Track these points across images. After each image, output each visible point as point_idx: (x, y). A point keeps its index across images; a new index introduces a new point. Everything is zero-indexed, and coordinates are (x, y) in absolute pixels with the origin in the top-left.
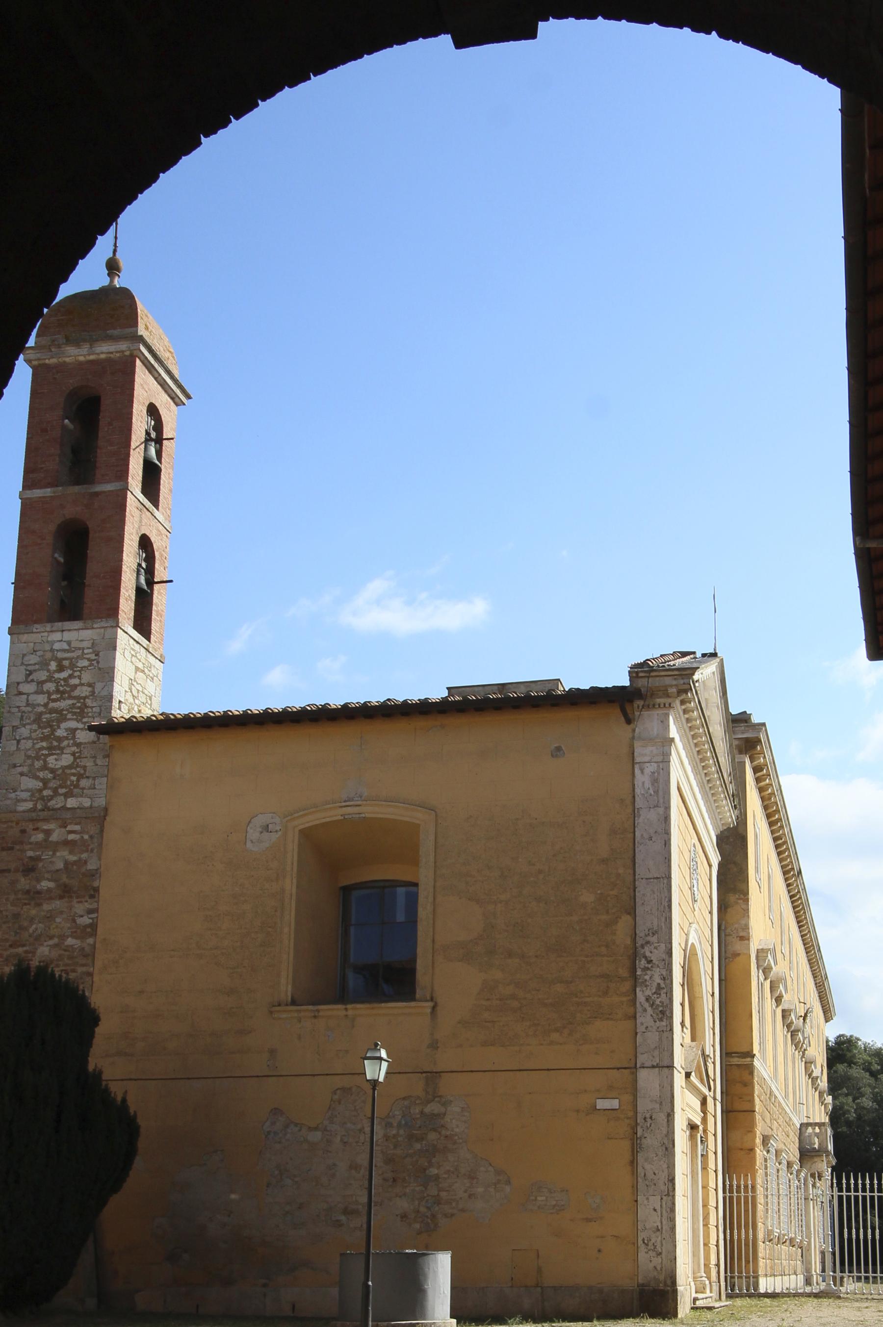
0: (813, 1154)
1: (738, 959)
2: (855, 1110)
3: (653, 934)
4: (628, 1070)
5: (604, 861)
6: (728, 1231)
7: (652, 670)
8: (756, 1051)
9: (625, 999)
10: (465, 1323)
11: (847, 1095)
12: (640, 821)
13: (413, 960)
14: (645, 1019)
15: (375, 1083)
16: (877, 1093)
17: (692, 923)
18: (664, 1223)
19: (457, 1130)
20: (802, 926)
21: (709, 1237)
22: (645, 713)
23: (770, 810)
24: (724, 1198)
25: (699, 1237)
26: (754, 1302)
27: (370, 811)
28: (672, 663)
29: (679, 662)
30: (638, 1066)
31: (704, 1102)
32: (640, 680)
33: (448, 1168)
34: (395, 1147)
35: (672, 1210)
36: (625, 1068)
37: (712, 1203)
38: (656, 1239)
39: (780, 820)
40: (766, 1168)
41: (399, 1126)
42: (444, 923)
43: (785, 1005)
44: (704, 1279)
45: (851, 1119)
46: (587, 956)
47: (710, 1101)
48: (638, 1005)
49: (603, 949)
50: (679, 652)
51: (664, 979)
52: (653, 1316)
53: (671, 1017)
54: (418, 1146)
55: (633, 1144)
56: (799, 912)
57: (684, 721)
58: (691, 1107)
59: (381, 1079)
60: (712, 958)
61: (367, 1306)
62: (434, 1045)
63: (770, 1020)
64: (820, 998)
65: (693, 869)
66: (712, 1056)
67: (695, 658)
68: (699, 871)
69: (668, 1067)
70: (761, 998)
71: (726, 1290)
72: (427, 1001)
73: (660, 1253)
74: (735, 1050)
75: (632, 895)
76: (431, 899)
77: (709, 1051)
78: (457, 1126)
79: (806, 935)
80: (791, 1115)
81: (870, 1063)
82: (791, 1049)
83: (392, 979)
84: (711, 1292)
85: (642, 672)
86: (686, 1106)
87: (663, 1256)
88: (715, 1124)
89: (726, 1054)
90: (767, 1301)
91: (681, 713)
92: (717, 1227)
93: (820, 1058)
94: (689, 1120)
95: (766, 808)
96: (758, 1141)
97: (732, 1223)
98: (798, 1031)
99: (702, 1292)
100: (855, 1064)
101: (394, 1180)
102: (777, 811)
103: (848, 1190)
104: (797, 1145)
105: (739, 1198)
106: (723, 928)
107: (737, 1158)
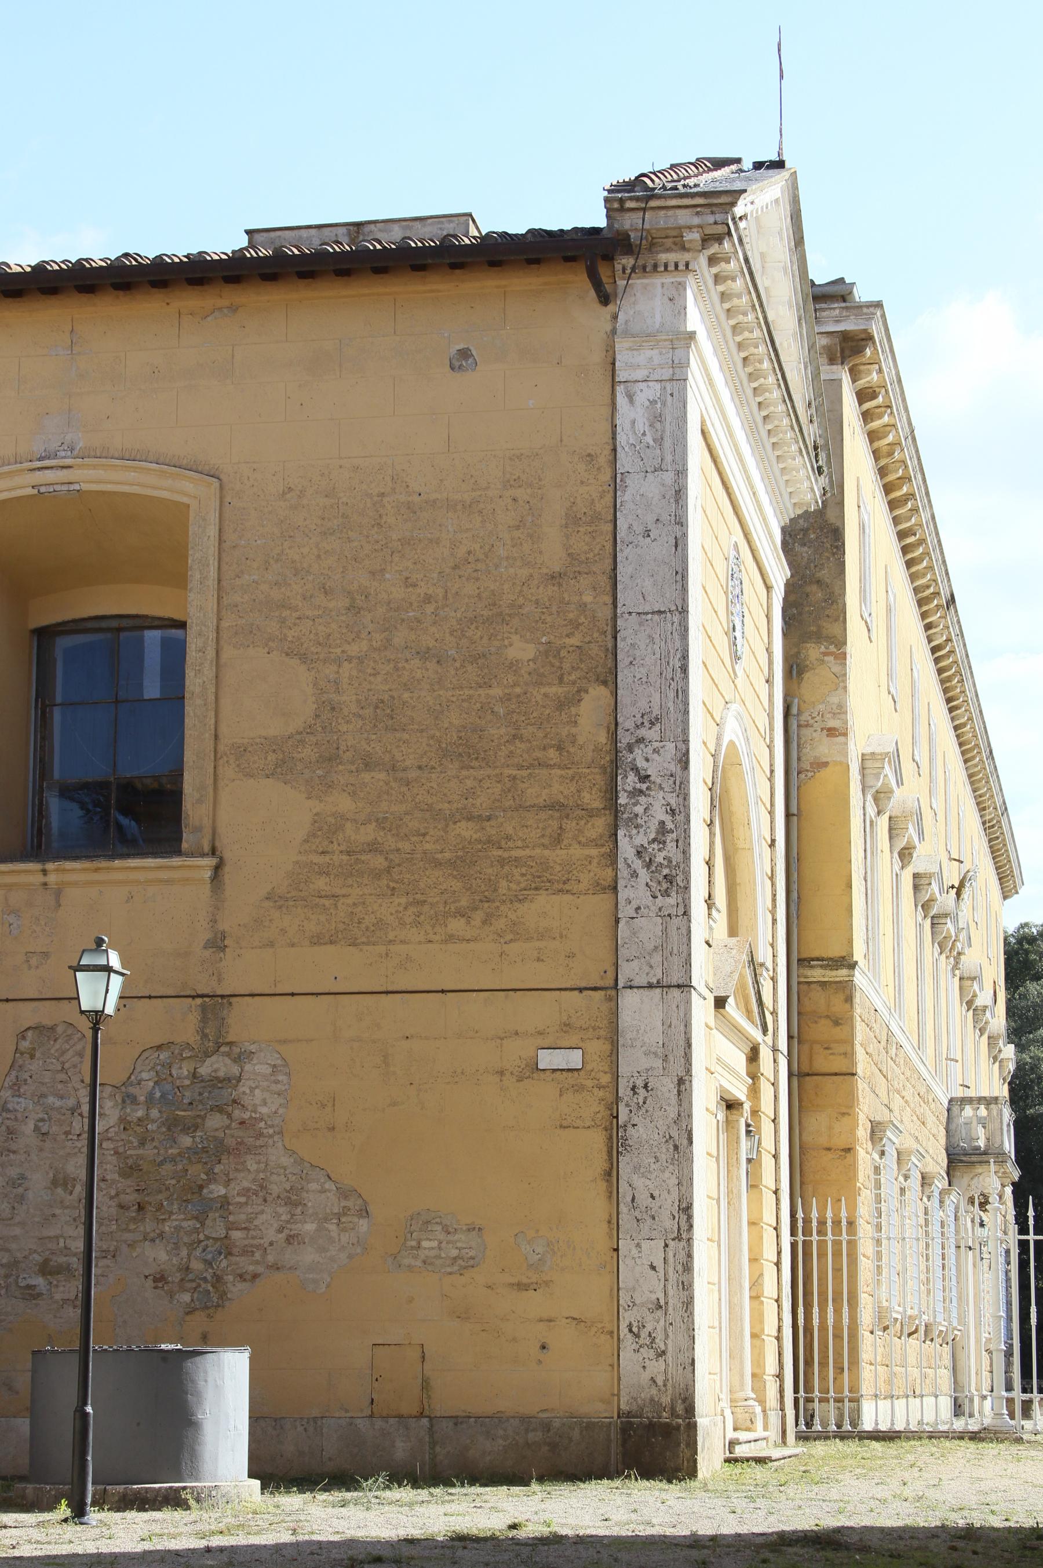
0: (974, 1158)
1: (824, 773)
3: (652, 723)
4: (602, 993)
5: (555, 578)
6: (801, 1310)
7: (651, 195)
8: (858, 955)
9: (594, 852)
10: (278, 1487)
12: (625, 497)
13: (178, 775)
14: (635, 891)
15: (97, 1017)
17: (728, 701)
18: (671, 1292)
19: (264, 1110)
20: (956, 708)
21: (762, 1322)
22: (637, 282)
24: (794, 1246)
26: (852, 1447)
27: (90, 478)
28: (691, 182)
29: (706, 181)
30: (621, 984)
31: (753, 1056)
32: (627, 215)
33: (246, 1184)
34: (142, 1144)
36: (595, 989)
38: (654, 1323)
40: (878, 1185)
43: (918, 864)
44: (751, 1402)
46: (520, 767)
47: (765, 1054)
48: (621, 865)
49: (552, 753)
50: (709, 160)
52: (647, 1474)
53: (687, 888)
54: (186, 1141)
55: (611, 1138)
57: (716, 299)
58: (727, 1067)
59: (110, 1010)
60: (772, 771)
61: (84, 1453)
62: (218, 943)
63: (888, 894)
64: (993, 850)
65: (735, 598)
67: (742, 171)
69: (679, 986)
71: (797, 1425)
72: (203, 855)
73: (664, 1353)
74: (816, 954)
75: (610, 645)
76: (211, 653)
77: (764, 955)
78: (265, 1103)
79: (964, 725)
80: (930, 1080)
82: (930, 951)
83: (139, 814)
85: (631, 199)
86: (716, 1062)
87: (669, 1354)
88: (775, 1098)
89: (799, 961)
91: (710, 281)
93: (993, 971)
94: (723, 1089)
95: (882, 472)
96: (863, 1132)
97: (808, 1294)
99: (748, 1429)
101: (141, 1208)
102: (906, 479)
104: (943, 1140)
105: (822, 1244)
106: (794, 710)
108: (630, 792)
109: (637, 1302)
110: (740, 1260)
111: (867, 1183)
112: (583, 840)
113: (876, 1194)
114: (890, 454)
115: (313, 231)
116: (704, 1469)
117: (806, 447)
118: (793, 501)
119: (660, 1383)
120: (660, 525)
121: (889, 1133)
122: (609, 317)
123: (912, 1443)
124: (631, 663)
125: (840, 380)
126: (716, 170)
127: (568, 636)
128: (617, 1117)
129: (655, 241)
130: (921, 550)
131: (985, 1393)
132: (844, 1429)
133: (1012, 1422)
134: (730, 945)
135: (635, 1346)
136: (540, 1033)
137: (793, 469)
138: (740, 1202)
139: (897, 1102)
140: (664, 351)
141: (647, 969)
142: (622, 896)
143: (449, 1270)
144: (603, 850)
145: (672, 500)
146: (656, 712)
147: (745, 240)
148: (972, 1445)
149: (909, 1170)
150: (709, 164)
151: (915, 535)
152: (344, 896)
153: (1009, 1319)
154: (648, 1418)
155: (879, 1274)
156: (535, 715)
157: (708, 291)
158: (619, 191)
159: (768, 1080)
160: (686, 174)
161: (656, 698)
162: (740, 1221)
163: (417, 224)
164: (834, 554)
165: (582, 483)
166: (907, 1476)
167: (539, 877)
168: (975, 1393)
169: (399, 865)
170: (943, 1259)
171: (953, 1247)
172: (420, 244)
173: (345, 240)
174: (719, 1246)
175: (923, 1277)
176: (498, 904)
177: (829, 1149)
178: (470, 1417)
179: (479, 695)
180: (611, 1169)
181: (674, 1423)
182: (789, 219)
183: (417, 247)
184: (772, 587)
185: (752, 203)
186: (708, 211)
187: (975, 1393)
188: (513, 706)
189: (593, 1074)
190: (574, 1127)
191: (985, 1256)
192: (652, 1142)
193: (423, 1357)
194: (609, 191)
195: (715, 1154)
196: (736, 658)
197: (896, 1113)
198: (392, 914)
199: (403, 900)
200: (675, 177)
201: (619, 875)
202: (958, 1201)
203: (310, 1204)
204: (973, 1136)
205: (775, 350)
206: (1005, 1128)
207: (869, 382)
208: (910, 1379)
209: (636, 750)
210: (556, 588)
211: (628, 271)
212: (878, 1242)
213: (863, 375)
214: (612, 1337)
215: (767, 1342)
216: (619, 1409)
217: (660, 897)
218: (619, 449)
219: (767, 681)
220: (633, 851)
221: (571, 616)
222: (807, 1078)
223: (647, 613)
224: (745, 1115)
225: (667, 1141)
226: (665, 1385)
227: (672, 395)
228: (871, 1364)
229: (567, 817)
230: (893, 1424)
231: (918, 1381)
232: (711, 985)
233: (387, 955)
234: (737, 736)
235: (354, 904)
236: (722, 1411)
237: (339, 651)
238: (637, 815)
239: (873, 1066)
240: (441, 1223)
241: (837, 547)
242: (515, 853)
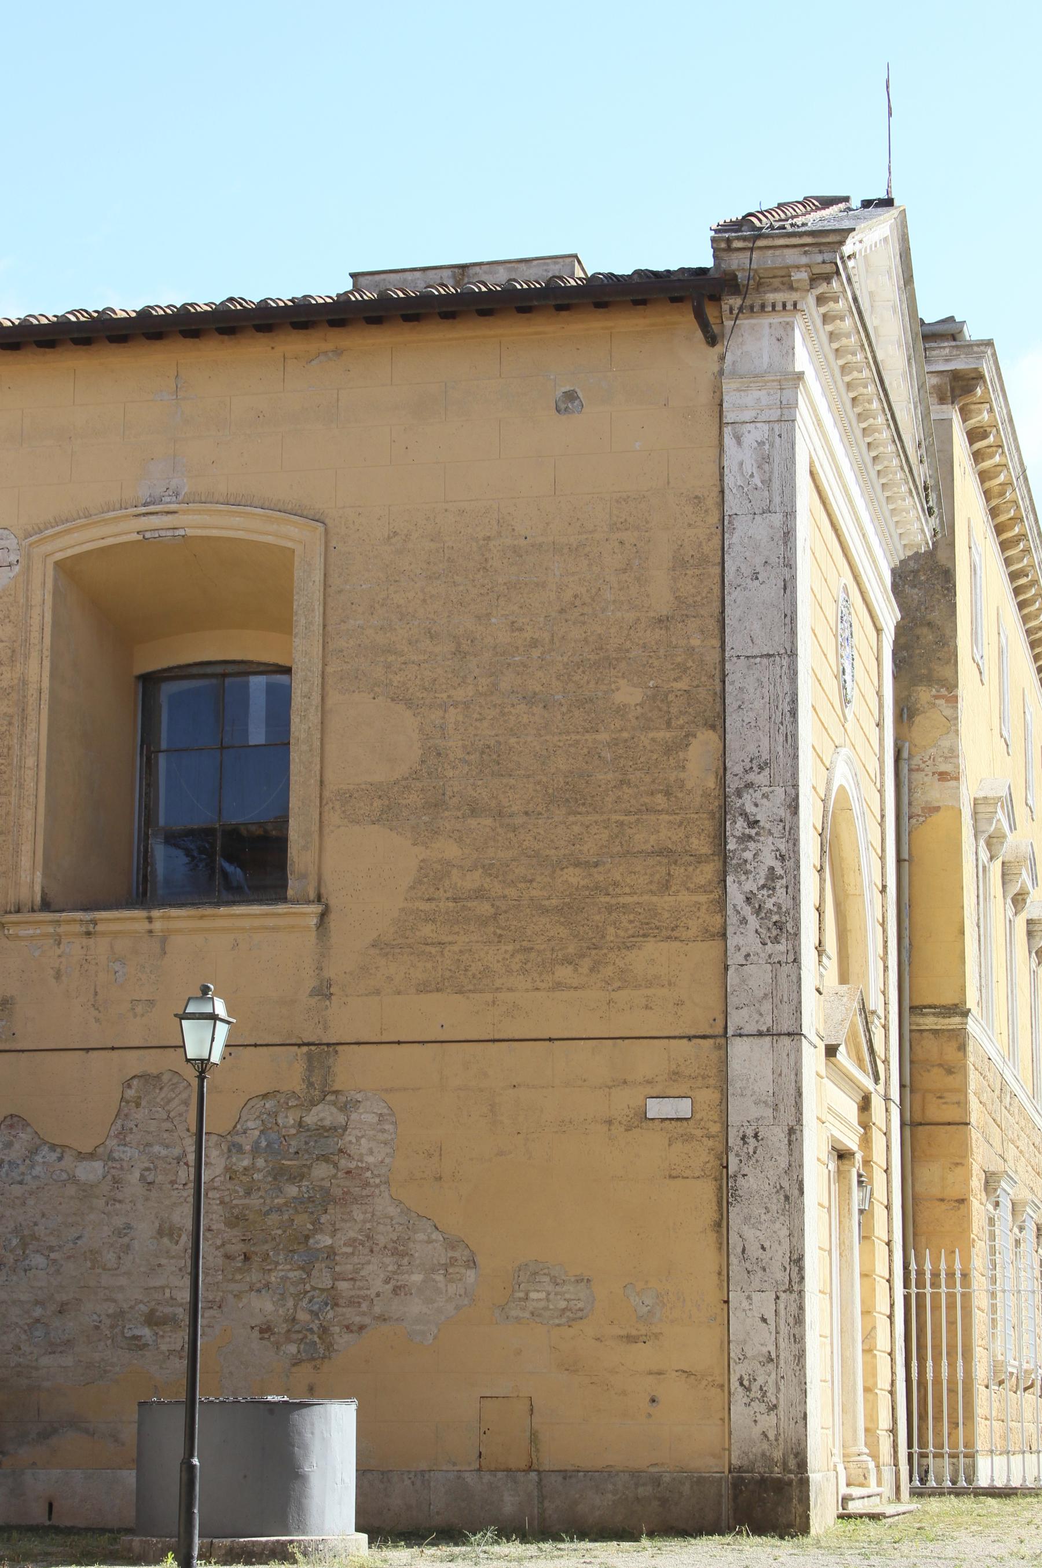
1: (936, 818)
3: (761, 768)
4: (711, 1041)
5: (662, 622)
6: (914, 1363)
7: (758, 234)
8: (971, 1003)
9: (703, 898)
10: (386, 1542)
13: (283, 822)
14: (744, 938)
15: (203, 1066)
17: (838, 746)
18: (782, 1345)
19: (370, 1159)
21: (874, 1375)
22: (745, 322)
23: (1003, 518)
24: (907, 1298)
26: (967, 1503)
27: (195, 523)
28: (799, 221)
29: (814, 220)
30: (730, 1032)
31: (865, 1105)
33: (352, 1234)
35: (799, 1320)
36: (704, 1037)
38: (765, 1377)
39: (1023, 536)
40: (992, 1237)
41: (256, 1150)
42: (342, 748)
44: (865, 1458)
46: (628, 813)
47: (877, 1104)
48: (730, 911)
49: (660, 799)
50: (817, 198)
51: (782, 858)
52: (759, 1529)
53: (797, 935)
54: (292, 1191)
55: (720, 1188)
57: (825, 339)
58: (837, 1116)
59: (216, 1058)
60: (883, 816)
62: (323, 991)
65: (844, 640)
66: (881, 1012)
67: (851, 209)
68: (855, 640)
69: (789, 1034)
71: (911, 1481)
72: (309, 902)
73: (775, 1407)
75: (718, 689)
77: (875, 1002)
78: (371, 1152)
83: (245, 861)
84: (879, 1484)
85: (738, 238)
86: (827, 1110)
87: (781, 1408)
88: (887, 1148)
89: (911, 1008)
90: (990, 1501)
91: (819, 321)
95: (994, 512)
96: (976, 1183)
97: (922, 1347)
101: (247, 1258)
102: (1018, 519)
105: (935, 1297)
106: (905, 754)
108: (739, 837)
110: (852, 1313)
111: (981, 1235)
112: (692, 886)
113: (991, 1246)
114: (1002, 494)
115: (418, 274)
117: (916, 488)
118: (903, 542)
119: (772, 1437)
120: (769, 568)
121: (1003, 1184)
122: (716, 358)
123: (1029, 1499)
125: (951, 420)
126: (824, 209)
127: (675, 680)
128: (727, 1167)
130: (1033, 591)
132: (959, 1485)
134: (841, 993)
135: (746, 1400)
136: (648, 1082)
137: (903, 510)
138: (852, 1254)
139: (1011, 1152)
141: (756, 1017)
142: (731, 942)
143: (557, 1321)
144: (712, 896)
145: (781, 542)
146: (765, 756)
147: (854, 279)
149: (1024, 1221)
150: (816, 203)
151: (1027, 576)
152: (450, 943)
154: (759, 1473)
155: (994, 1327)
156: (642, 760)
157: (817, 332)
158: (726, 231)
159: (880, 1130)
160: (794, 213)
161: (765, 742)
162: (852, 1272)
163: (523, 266)
164: (945, 596)
165: (690, 525)
166: (1023, 1533)
167: (647, 924)
169: (506, 912)
172: (525, 286)
173: (450, 282)
174: (831, 1298)
176: (606, 951)
177: (942, 1200)
178: (579, 1471)
180: (721, 1219)
181: (786, 1478)
182: (898, 257)
183: (523, 289)
185: (861, 242)
188: (621, 751)
189: (702, 1123)
190: (683, 1178)
192: (762, 1192)
193: (532, 1410)
194: (716, 231)
195: (827, 1205)
197: (1011, 1163)
198: (498, 961)
199: (510, 948)
200: (783, 216)
203: (417, 1255)
205: (885, 390)
209: (745, 795)
210: (663, 632)
211: (736, 312)
213: (974, 415)
214: (723, 1391)
216: (730, 1464)
217: (770, 944)
218: (727, 491)
219: (878, 725)
220: (742, 897)
221: (679, 659)
222: (920, 1128)
223: (755, 657)
224: (857, 1165)
225: (777, 1192)
226: (777, 1440)
227: (780, 436)
228: (986, 1419)
229: (675, 862)
230: (1009, 1480)
231: (1035, 1437)
232: (822, 1034)
233: (494, 1002)
234: (847, 780)
235: (461, 951)
236: (835, 1466)
237: (444, 696)
238: (746, 861)
240: (548, 1274)
241: (947, 589)
242: (622, 900)
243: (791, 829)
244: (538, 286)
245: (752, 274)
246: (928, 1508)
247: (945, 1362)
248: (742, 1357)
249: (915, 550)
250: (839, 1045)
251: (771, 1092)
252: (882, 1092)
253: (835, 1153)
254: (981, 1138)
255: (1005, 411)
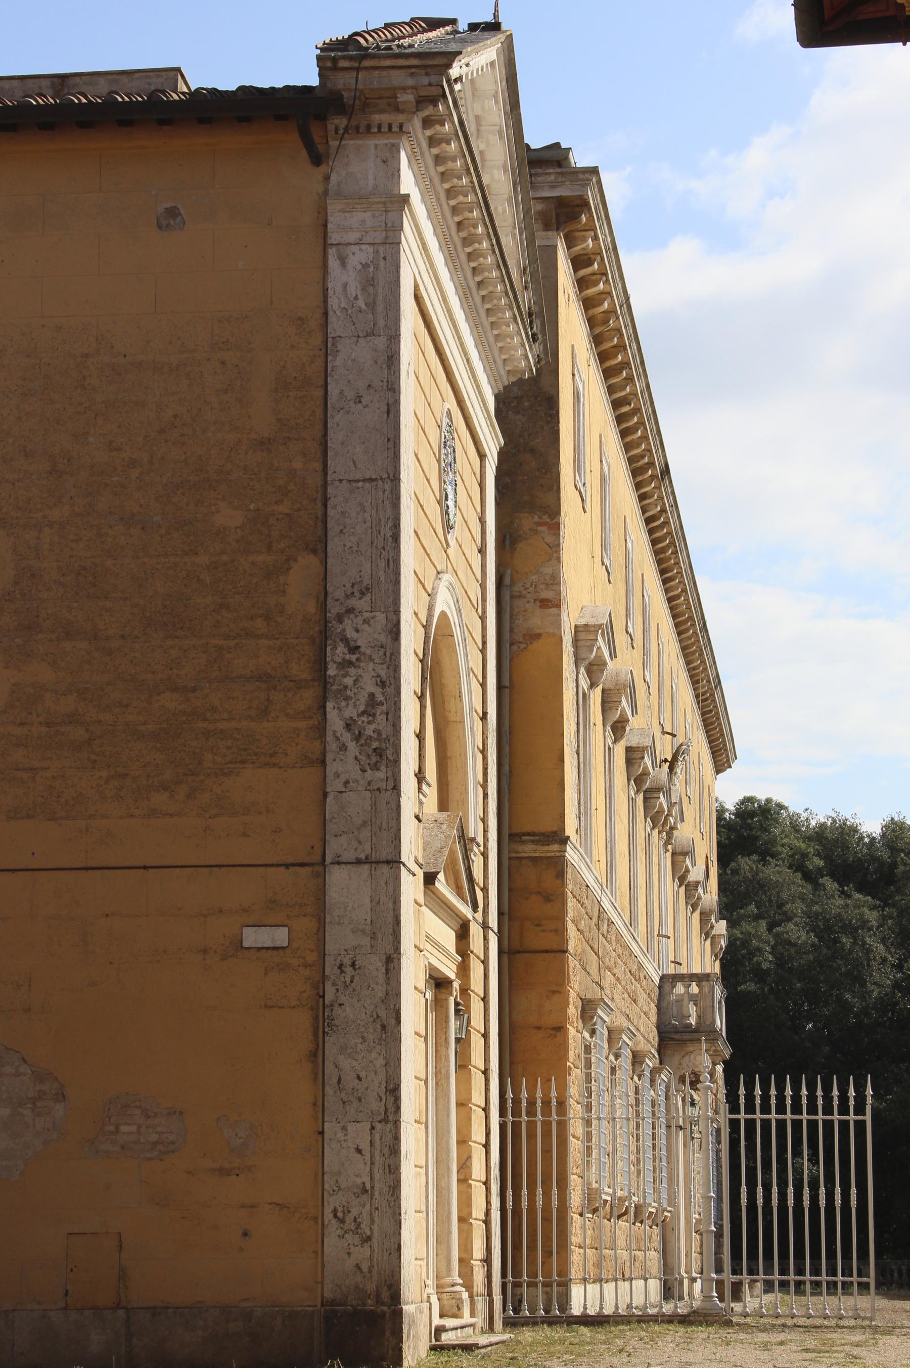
0: (686, 1036)
1: (537, 645)
2: (773, 948)
3: (363, 594)
4: (309, 869)
6: (510, 1192)
7: (365, 54)
9: (302, 724)
11: (757, 918)
12: (337, 362)
14: (344, 765)
16: (817, 914)
18: (377, 1176)
21: (469, 1205)
22: (350, 143)
23: (606, 346)
25: (449, 1203)
26: (558, 1333)
28: (406, 42)
30: (328, 860)
31: (463, 934)
35: (394, 1150)
36: (302, 865)
37: (478, 1135)
39: (626, 364)
40: (588, 1065)
43: (632, 738)
44: (458, 1288)
45: (765, 966)
47: (475, 931)
49: (259, 623)
50: (423, 20)
51: (383, 684)
53: (397, 762)
55: (316, 1018)
56: (663, 550)
57: (430, 162)
60: (484, 643)
65: (447, 465)
67: (456, 32)
68: (458, 465)
69: (388, 862)
70: (583, 725)
71: (504, 1310)
73: (369, 1238)
74: (528, 828)
75: (320, 513)
77: (474, 829)
79: (678, 597)
80: (641, 958)
81: (804, 856)
82: (642, 826)
84: (473, 1314)
85: (344, 58)
86: (424, 938)
87: (374, 1240)
88: (486, 978)
89: (509, 836)
90: (584, 1330)
91: (424, 144)
92: (487, 1183)
93: (705, 848)
95: (597, 340)
96: (573, 1011)
98: (659, 790)
99: (455, 1316)
100: (772, 856)
103: (750, 1109)
104: (654, 1019)
105: (531, 1125)
106: (507, 581)
107: (529, 1046)
108: (339, 663)
109: (343, 1186)
110: (448, 1142)
111: (578, 1063)
113: (586, 1074)
114: (606, 322)
115: (16, 83)
116: (409, 1358)
118: (507, 368)
119: (365, 1269)
121: (599, 1011)
122: (320, 178)
123: (621, 1327)
124: (341, 531)
127: (276, 503)
128: (323, 996)
129: (368, 101)
130: (636, 419)
131: (694, 1275)
133: (721, 1305)
135: (339, 1232)
136: (245, 910)
137: (508, 336)
139: (608, 979)
140: (377, 214)
141: (355, 844)
142: (331, 769)
143: (148, 1155)
144: (311, 722)
145: (384, 366)
146: (367, 581)
147: (460, 103)
148: (681, 1330)
149: (620, 1048)
151: (630, 404)
152: (42, 769)
153: (719, 1199)
154: (352, 1306)
155: (589, 1154)
157: (422, 154)
158: (332, 50)
159: (478, 958)
161: (367, 567)
162: (449, 1102)
163: (124, 79)
164: (548, 422)
165: (292, 347)
167: (245, 750)
168: (685, 1275)
170: (654, 1139)
171: (663, 1126)
172: (127, 99)
173: (48, 92)
174: (427, 1128)
175: (633, 1158)
177: (539, 1028)
178: (168, 1308)
179: (185, 563)
180: (317, 1050)
181: (379, 1311)
182: (504, 82)
183: (124, 102)
184: (485, 455)
185: (467, 65)
186: (423, 72)
187: (685, 1275)
191: (697, 1135)
193: (121, 1246)
194: (322, 49)
195: (424, 1034)
196: (448, 527)
197: (608, 991)
199: (104, 774)
201: (328, 749)
202: (669, 1080)
204: (684, 1012)
206: (717, 1006)
207: (584, 249)
208: (619, 1262)
209: (346, 621)
211: (341, 132)
212: (588, 1123)
214: (317, 1223)
215: (474, 1226)
216: (323, 1297)
217: (369, 771)
218: (331, 313)
219: (480, 551)
222: (518, 956)
223: (358, 481)
224: (455, 993)
225: (374, 1021)
226: (370, 1272)
227: (385, 258)
228: (580, 1247)
229: (275, 688)
230: (601, 1308)
231: (628, 1264)
232: (421, 861)
233: (87, 830)
234: (449, 607)
238: (346, 687)
239: (585, 943)
241: (550, 416)
243: (391, 655)
244: (140, 99)
245: (358, 94)
246: (520, 1338)
247: (540, 1190)
248: (336, 1189)
249: (519, 376)
250: (438, 873)
251: (369, 920)
252: (480, 920)
253: (432, 982)
254: (578, 966)
255: (609, 239)
